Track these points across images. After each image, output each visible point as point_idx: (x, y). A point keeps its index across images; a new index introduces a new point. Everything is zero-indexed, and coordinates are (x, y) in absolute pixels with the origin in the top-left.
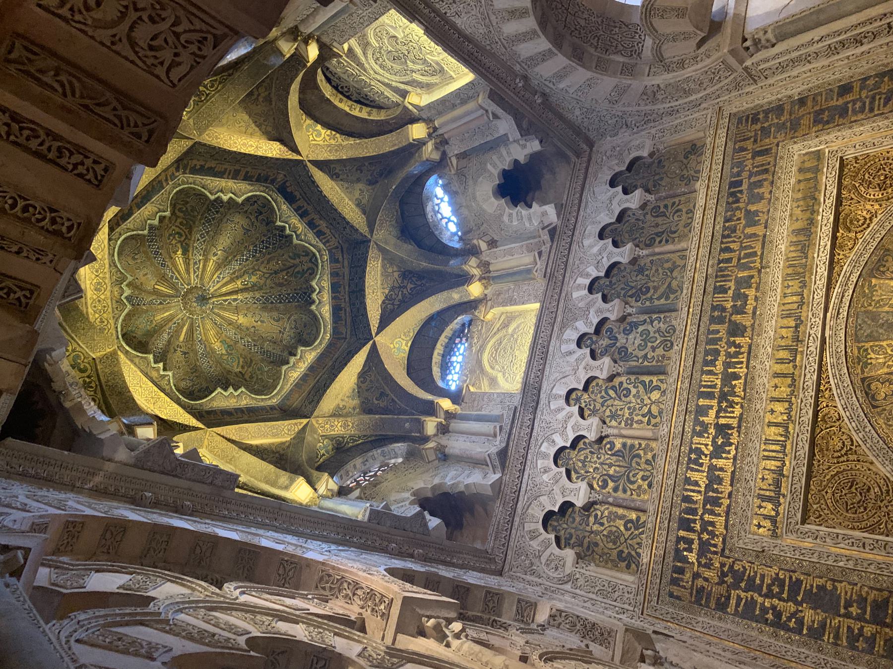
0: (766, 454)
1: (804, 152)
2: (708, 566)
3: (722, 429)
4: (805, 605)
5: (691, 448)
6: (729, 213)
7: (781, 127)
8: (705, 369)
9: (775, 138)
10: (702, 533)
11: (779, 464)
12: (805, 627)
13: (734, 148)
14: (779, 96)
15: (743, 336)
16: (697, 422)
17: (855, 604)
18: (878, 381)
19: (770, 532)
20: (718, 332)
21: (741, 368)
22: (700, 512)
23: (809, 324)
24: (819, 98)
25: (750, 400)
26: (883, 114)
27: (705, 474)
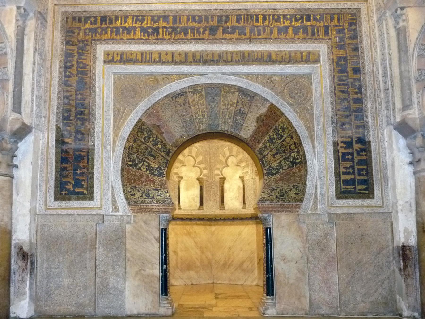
0: (144, 54)
1: (321, 53)
2: (85, 33)
3: (156, 31)
4: (77, 78)
5: (145, 16)
6: (289, 17)
7: (341, 39)
8: (190, 17)
9: (335, 37)
10: (101, 28)
11: (140, 60)
12: (68, 79)
13: (334, 14)
14: (364, 36)
15: (209, 35)
16: (159, 17)
17: (82, 97)
18: (185, 98)
19: (106, 60)
20: (213, 21)
21: (191, 36)
22: (111, 26)
23: (215, 66)
24: (355, 58)
25: (173, 43)
26: (335, 90)
27: (131, 25)
